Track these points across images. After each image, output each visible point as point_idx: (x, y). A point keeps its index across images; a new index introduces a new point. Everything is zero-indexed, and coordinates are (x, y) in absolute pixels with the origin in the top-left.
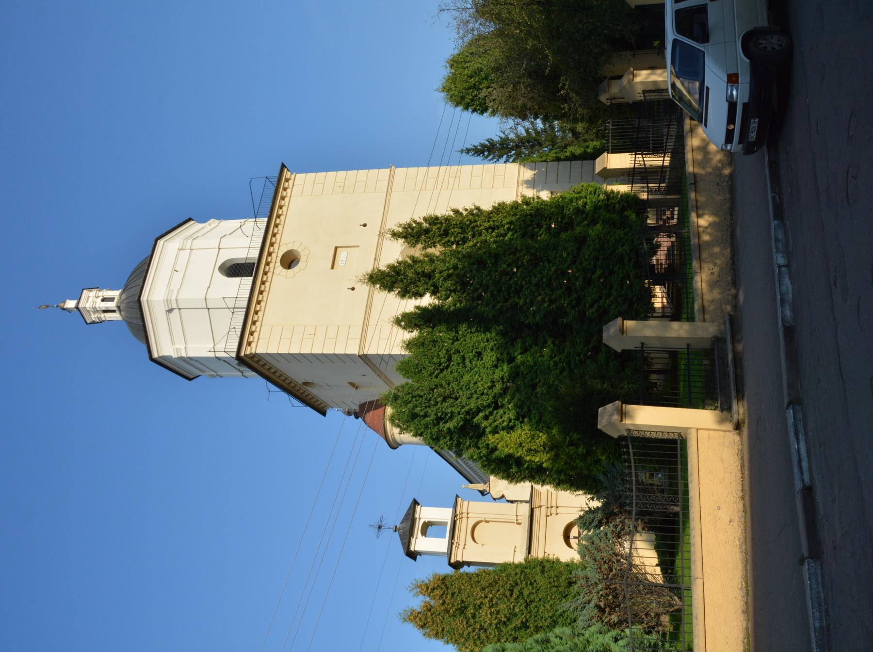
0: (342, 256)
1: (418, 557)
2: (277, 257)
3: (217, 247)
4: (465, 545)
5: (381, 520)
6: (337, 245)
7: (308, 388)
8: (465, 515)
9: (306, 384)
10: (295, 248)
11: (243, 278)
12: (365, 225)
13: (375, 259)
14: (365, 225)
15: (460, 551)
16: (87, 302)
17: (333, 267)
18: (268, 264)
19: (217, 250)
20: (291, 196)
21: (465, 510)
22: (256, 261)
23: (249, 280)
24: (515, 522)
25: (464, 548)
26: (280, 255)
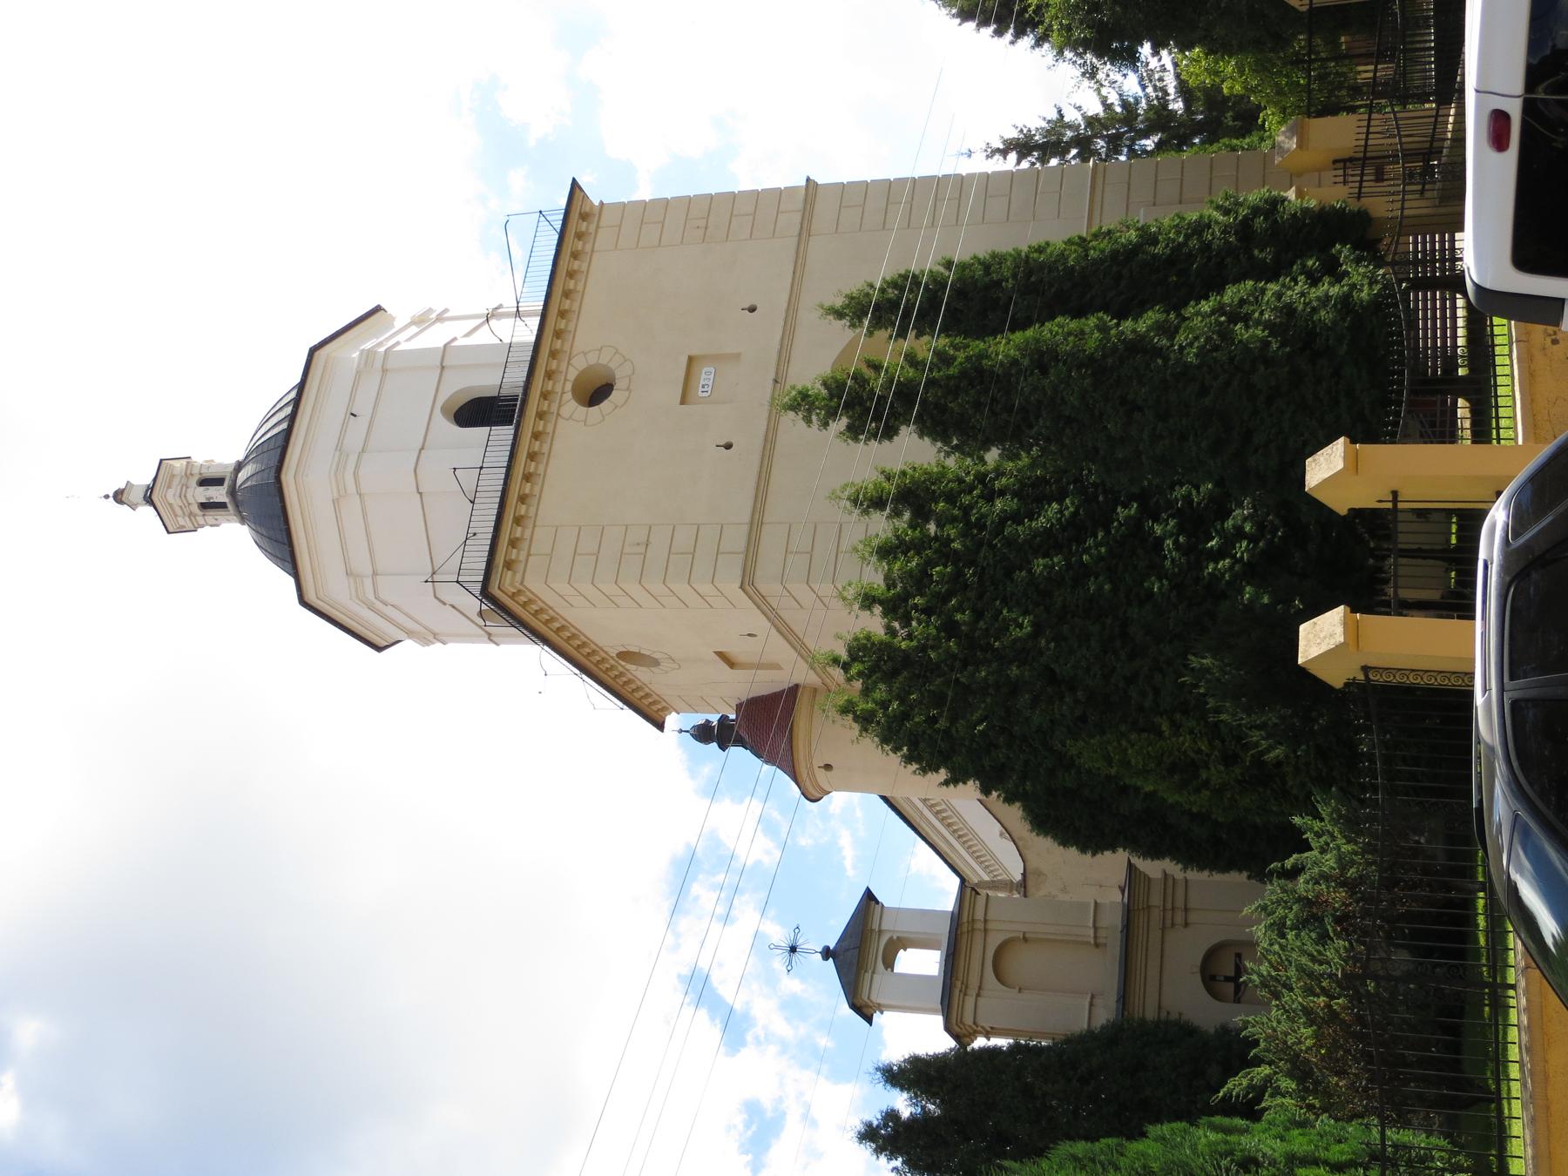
0: (703, 376)
1: (877, 1017)
2: (566, 380)
3: (439, 364)
4: (980, 988)
5: (796, 935)
6: (694, 352)
7: (629, 666)
8: (980, 926)
9: (625, 656)
10: (603, 361)
11: (493, 428)
12: (752, 309)
13: (776, 381)
14: (752, 309)
15: (970, 1002)
16: (169, 487)
17: (683, 402)
18: (545, 395)
20: (593, 251)
21: (979, 915)
22: (520, 391)
23: (505, 433)
24: (1092, 941)
25: (978, 995)
26: (572, 375)
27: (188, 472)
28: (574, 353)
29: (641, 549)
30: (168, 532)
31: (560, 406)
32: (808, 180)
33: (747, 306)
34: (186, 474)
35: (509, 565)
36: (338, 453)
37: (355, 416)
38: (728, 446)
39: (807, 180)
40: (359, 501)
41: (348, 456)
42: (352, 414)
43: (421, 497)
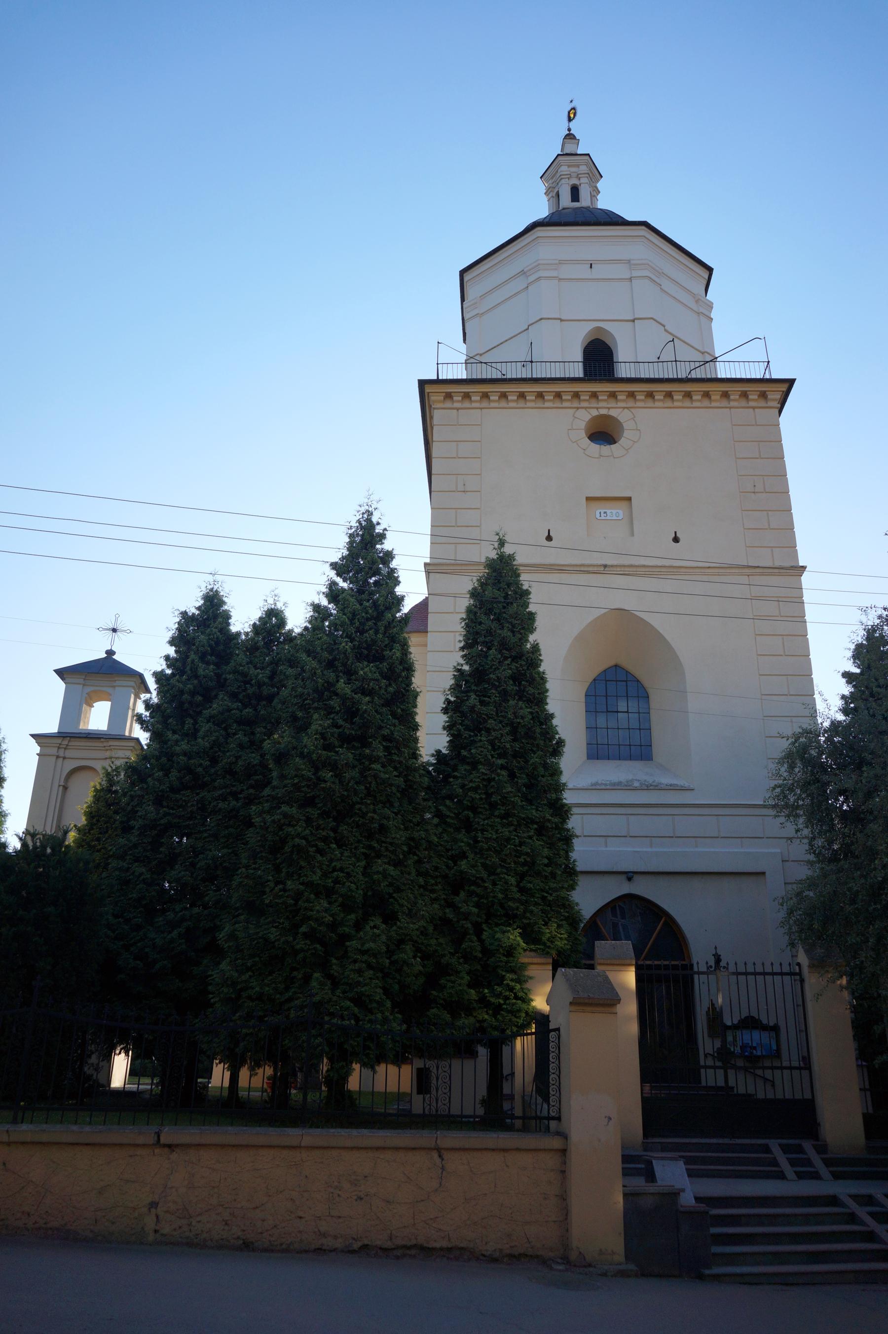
0: (614, 512)
2: (609, 408)
3: (637, 316)
5: (125, 631)
12: (676, 540)
13: (605, 566)
16: (569, 166)
19: (631, 318)
20: (730, 408)
26: (613, 413)
27: (580, 176)
28: (632, 410)
29: (461, 488)
30: (541, 178)
31: (586, 408)
32: (804, 568)
33: (678, 535)
34: (578, 175)
35: (449, 396)
36: (557, 262)
37: (591, 267)
38: (549, 538)
39: (802, 567)
40: (523, 288)
41: (556, 269)
42: (591, 264)
43: (525, 331)
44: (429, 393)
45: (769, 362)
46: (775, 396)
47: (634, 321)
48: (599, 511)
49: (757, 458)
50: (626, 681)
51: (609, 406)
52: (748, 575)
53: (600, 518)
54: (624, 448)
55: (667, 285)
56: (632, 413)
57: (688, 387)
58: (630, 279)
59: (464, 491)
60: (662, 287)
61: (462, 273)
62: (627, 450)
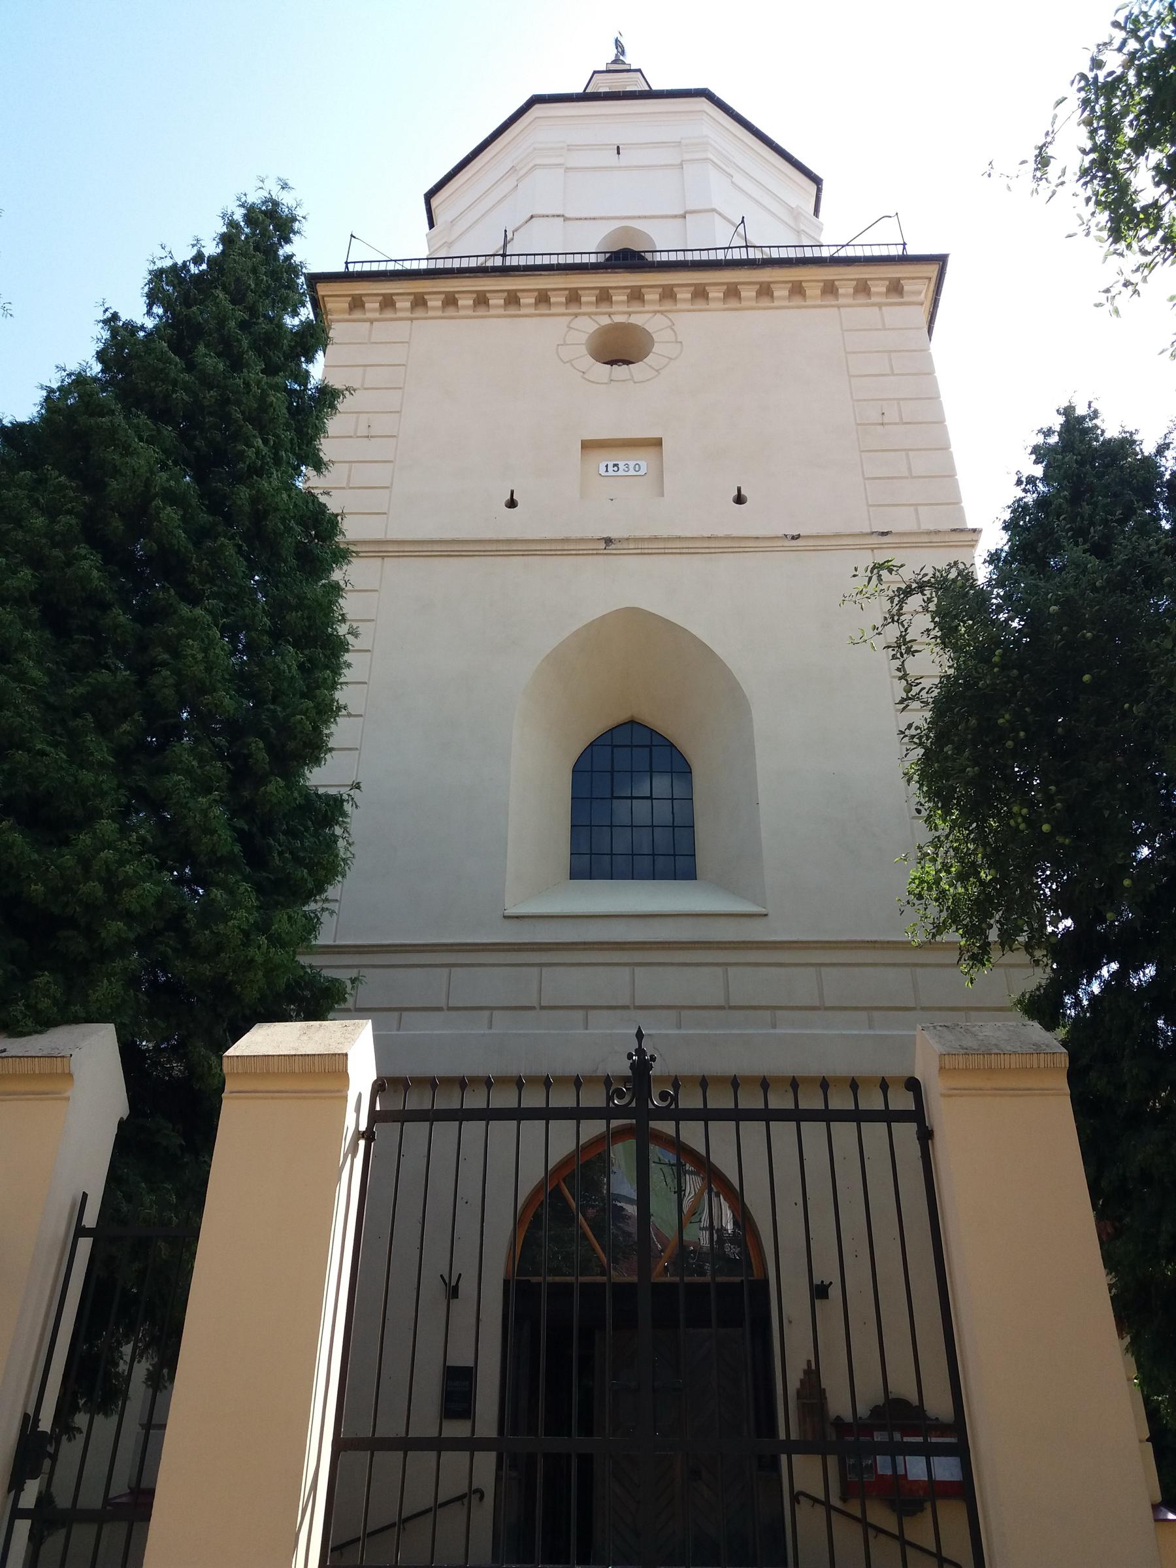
0: (632, 464)
2: (629, 314)
3: (690, 207)
12: (740, 499)
13: (608, 541)
17: (587, 445)
19: (681, 212)
20: (839, 307)
26: (636, 320)
28: (670, 315)
29: (362, 431)
31: (589, 314)
33: (743, 492)
38: (512, 504)
39: (974, 530)
42: (618, 148)
44: (323, 297)
45: (904, 244)
46: (918, 289)
47: (685, 217)
48: (602, 462)
49: (888, 375)
50: (650, 747)
51: (630, 309)
52: (872, 549)
53: (607, 474)
54: (653, 368)
55: (739, 179)
56: (670, 319)
57: (765, 275)
58: (681, 166)
59: (368, 437)
60: (733, 179)
61: (429, 196)
62: (657, 371)
